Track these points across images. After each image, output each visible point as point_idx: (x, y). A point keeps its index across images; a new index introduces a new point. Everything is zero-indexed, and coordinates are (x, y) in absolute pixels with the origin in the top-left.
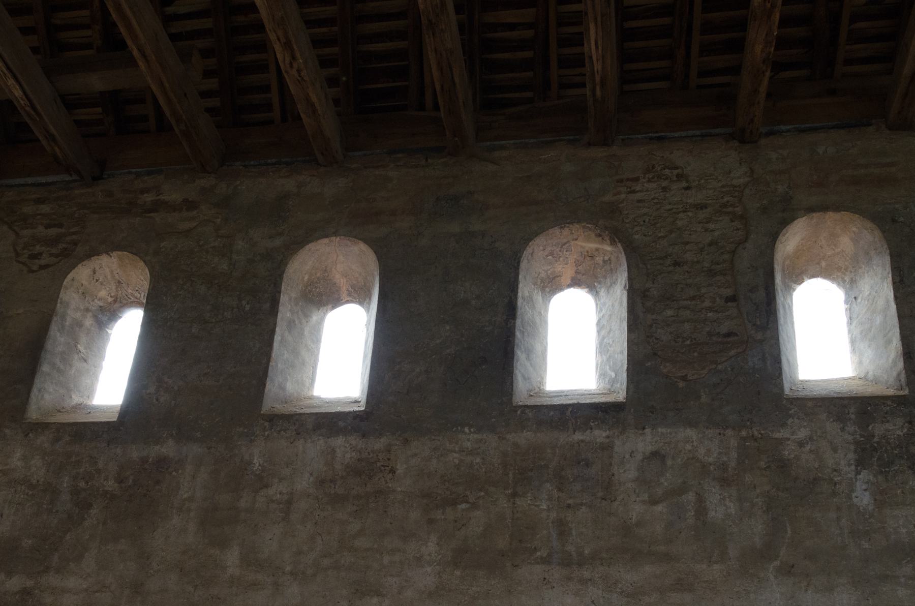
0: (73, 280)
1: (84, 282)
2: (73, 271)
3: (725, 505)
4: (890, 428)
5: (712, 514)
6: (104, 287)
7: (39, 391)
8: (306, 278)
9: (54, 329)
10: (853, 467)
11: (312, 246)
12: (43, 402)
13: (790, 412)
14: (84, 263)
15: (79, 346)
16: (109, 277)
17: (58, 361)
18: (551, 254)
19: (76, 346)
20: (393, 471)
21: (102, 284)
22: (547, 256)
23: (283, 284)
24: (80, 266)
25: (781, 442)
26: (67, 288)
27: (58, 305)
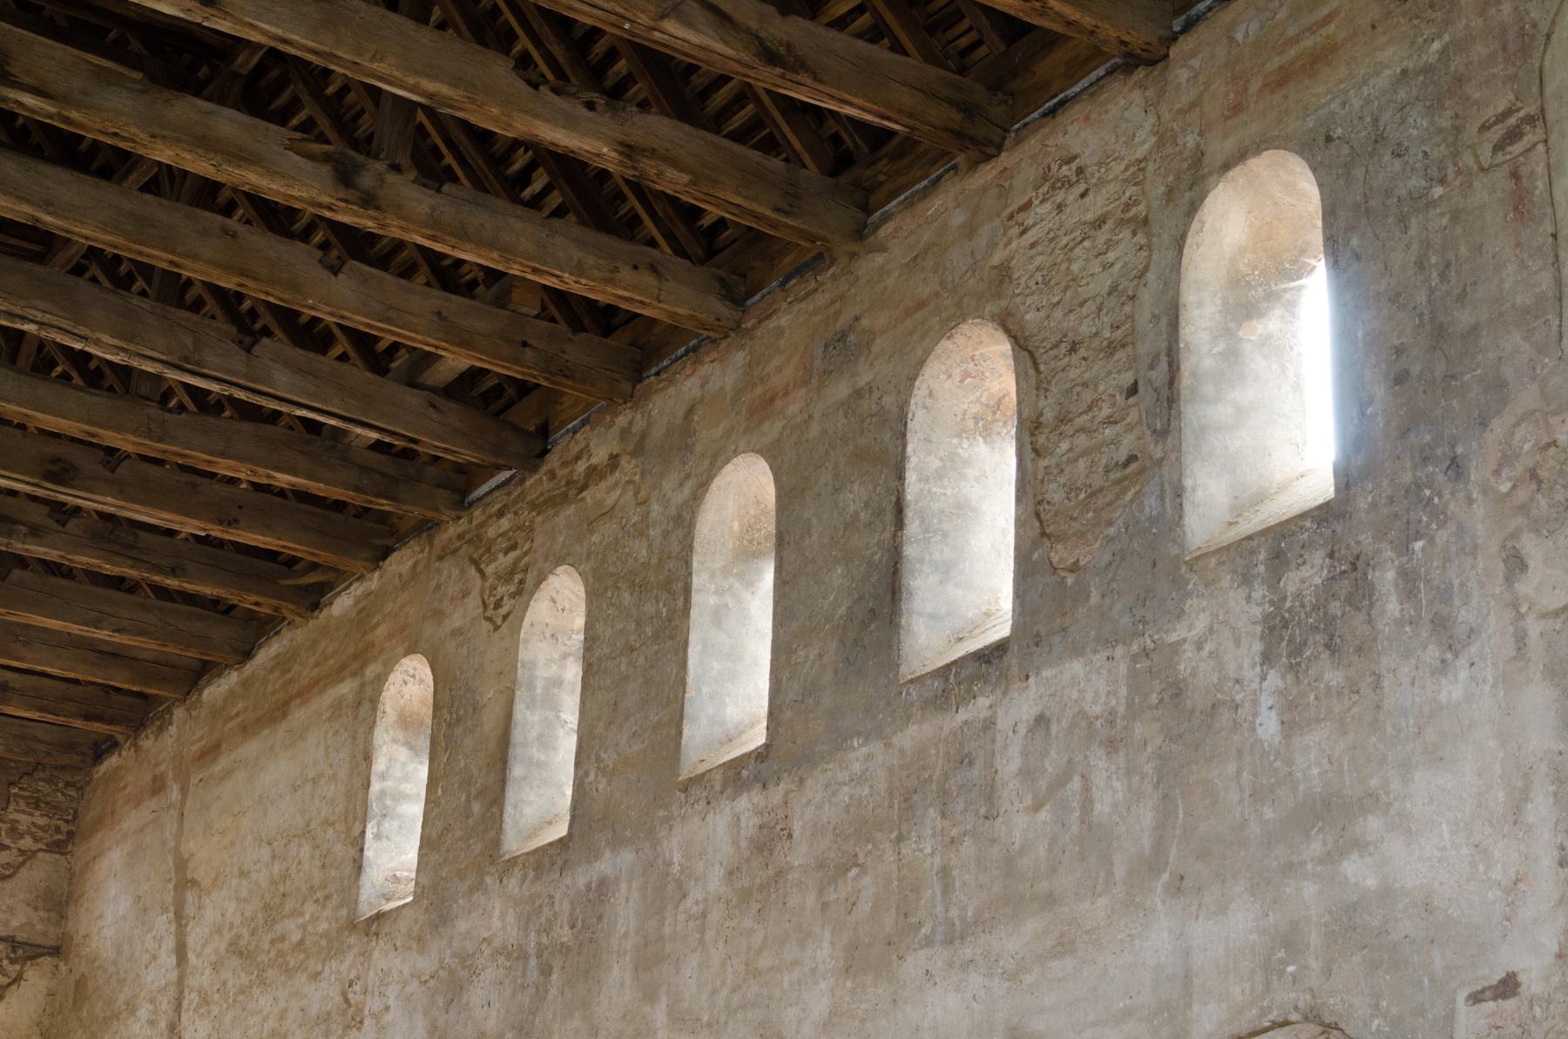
0: (532, 625)
1: (548, 621)
2: (528, 614)
3: (1112, 787)
4: (1307, 575)
5: (1098, 807)
6: (575, 614)
7: (515, 807)
8: (736, 526)
9: (520, 709)
10: (1258, 669)
11: (718, 482)
12: (524, 820)
13: (1189, 587)
14: (536, 596)
15: (562, 714)
16: (574, 598)
17: (536, 753)
18: (966, 375)
19: (558, 717)
20: (790, 836)
21: (571, 611)
22: (962, 381)
23: (694, 558)
24: (532, 603)
25: (1176, 648)
26: (526, 641)
27: (520, 671)
